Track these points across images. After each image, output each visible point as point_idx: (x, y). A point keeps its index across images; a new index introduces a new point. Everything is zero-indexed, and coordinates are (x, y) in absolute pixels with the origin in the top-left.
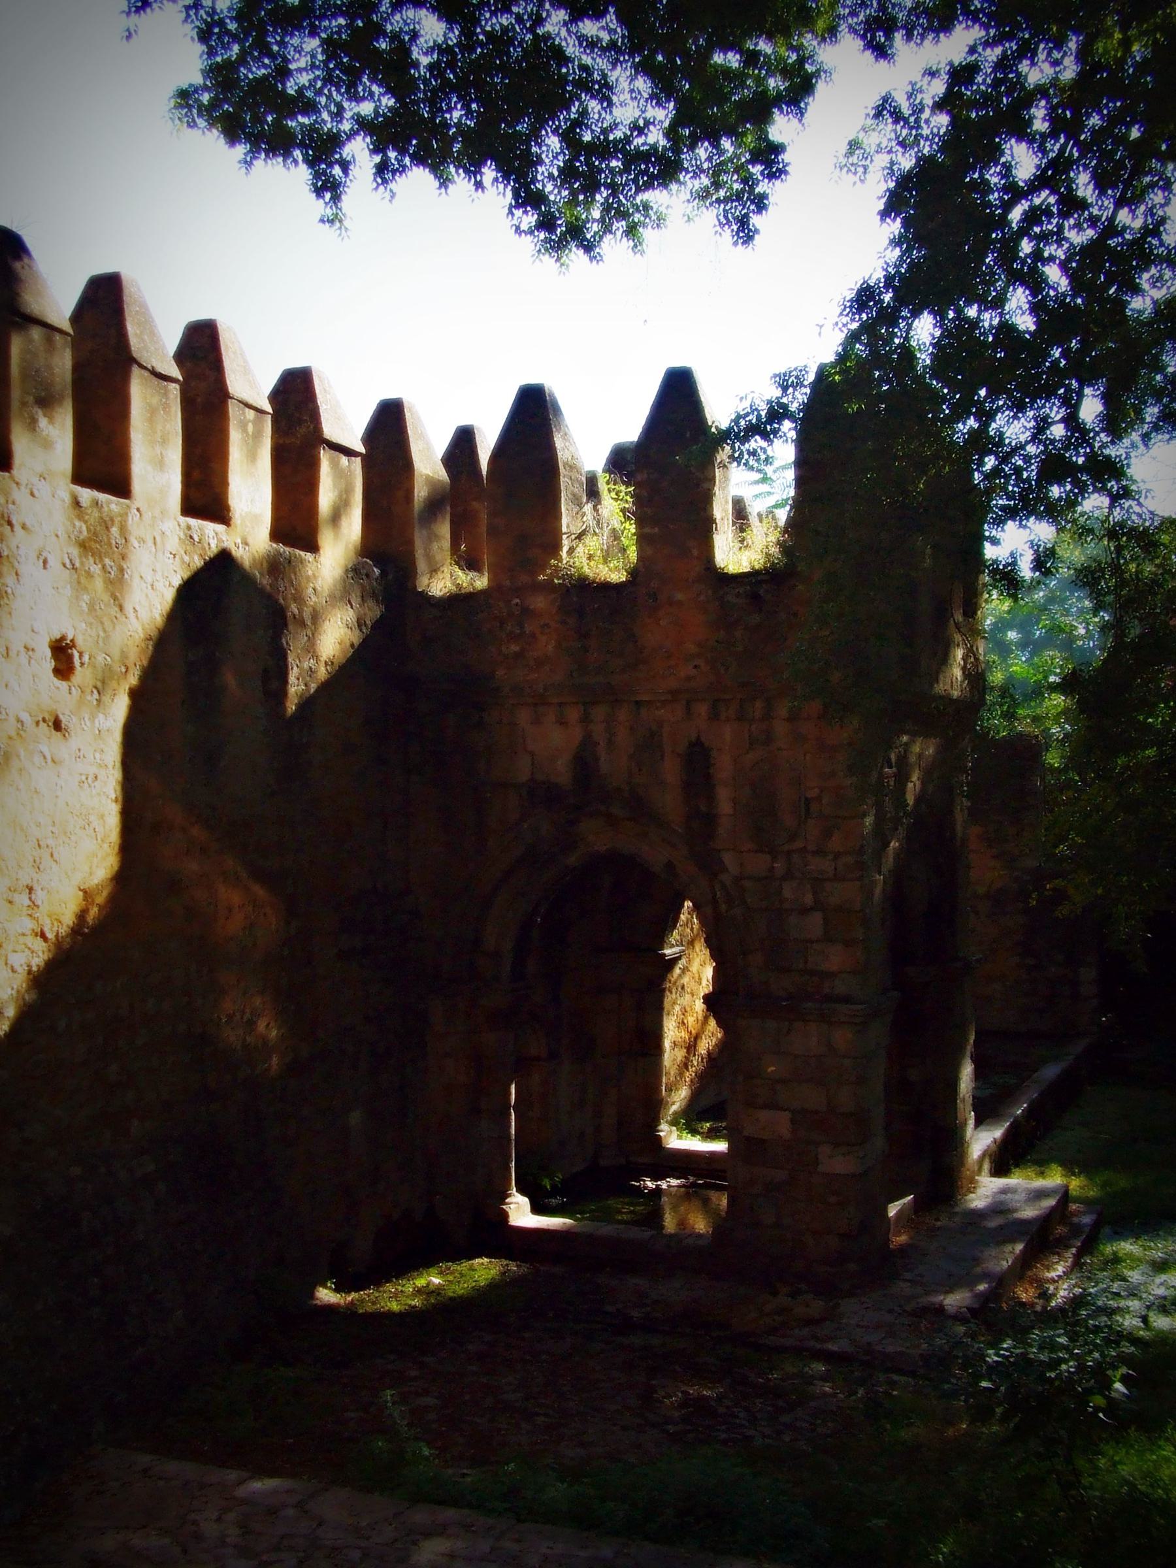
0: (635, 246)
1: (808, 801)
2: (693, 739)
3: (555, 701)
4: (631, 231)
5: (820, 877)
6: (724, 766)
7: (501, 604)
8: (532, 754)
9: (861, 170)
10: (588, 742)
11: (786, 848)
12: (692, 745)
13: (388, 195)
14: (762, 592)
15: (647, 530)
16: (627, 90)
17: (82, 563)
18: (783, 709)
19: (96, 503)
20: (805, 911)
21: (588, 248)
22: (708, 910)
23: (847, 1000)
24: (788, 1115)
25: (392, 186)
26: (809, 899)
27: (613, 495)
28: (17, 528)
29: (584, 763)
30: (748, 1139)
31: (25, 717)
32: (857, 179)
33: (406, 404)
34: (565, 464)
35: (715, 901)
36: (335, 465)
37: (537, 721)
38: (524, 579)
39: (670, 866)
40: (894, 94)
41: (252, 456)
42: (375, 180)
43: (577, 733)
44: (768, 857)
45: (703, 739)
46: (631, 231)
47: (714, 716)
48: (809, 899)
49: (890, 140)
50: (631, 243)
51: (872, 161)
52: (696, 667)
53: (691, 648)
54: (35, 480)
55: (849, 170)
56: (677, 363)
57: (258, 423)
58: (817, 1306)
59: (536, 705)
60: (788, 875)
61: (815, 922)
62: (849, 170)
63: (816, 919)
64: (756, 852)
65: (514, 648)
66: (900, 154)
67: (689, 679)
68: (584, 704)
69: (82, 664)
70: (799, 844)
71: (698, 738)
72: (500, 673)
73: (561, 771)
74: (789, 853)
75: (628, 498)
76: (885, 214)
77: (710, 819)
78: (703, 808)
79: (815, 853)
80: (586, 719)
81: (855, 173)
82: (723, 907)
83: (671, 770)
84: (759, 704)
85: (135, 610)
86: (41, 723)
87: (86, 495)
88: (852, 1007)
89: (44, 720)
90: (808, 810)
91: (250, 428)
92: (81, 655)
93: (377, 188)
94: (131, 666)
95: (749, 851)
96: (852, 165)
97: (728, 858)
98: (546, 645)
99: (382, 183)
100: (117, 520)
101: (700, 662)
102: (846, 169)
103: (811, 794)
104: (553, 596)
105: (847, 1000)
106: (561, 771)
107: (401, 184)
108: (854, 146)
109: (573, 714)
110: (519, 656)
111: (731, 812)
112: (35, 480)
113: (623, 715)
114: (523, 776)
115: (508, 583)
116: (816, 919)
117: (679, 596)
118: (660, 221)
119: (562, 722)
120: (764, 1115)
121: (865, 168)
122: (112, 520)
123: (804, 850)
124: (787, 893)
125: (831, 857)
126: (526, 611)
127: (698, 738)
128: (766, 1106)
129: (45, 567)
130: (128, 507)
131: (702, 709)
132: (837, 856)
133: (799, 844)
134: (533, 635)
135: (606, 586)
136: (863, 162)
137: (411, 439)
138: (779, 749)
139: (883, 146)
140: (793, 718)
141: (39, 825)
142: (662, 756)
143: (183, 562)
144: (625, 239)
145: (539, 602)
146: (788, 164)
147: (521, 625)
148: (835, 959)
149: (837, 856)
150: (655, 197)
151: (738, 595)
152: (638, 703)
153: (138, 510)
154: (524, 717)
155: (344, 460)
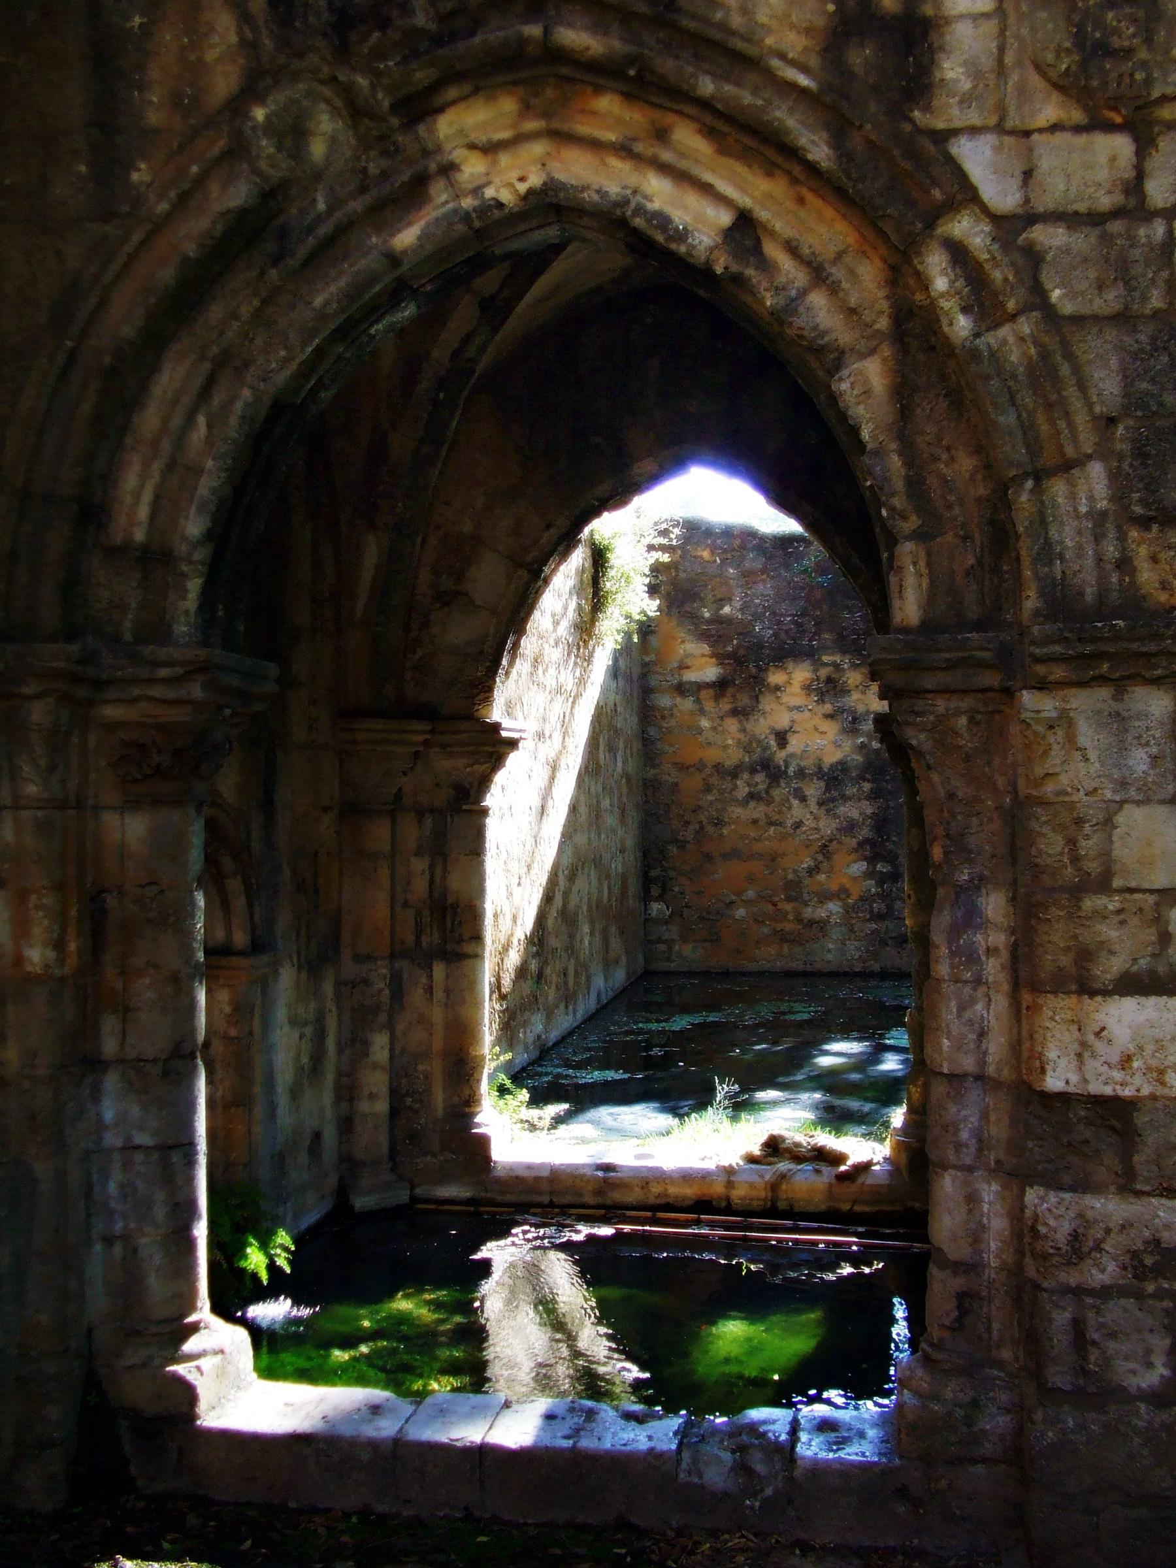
44: (1122, 145)
64: (1078, 129)
95: (1055, 128)
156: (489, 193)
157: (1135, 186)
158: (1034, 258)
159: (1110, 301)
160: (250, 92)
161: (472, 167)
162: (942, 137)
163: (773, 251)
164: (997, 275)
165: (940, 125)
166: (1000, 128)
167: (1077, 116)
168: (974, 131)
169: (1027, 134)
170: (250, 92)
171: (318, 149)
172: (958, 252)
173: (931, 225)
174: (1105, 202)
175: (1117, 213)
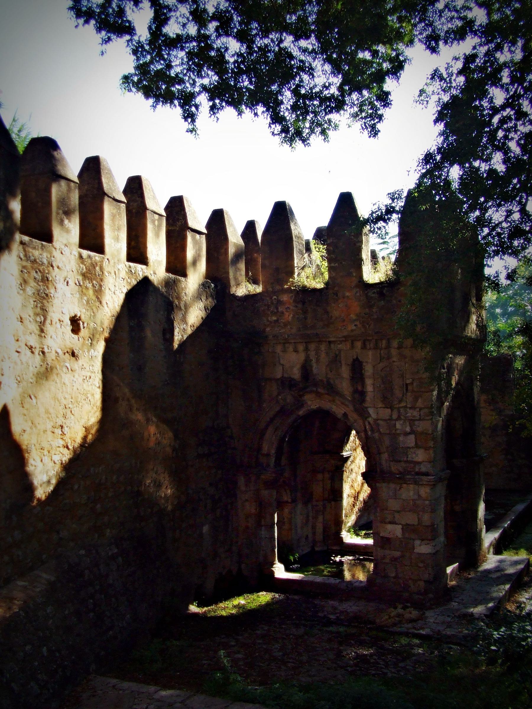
0: (325, 139)
1: (407, 385)
2: (355, 357)
3: (293, 341)
4: (323, 132)
5: (413, 418)
6: (368, 370)
7: (268, 299)
8: (283, 365)
9: (425, 102)
11: (397, 406)
12: (354, 360)
13: (216, 119)
14: (384, 291)
15: (332, 265)
16: (321, 70)
17: (84, 283)
19: (89, 257)
20: (406, 434)
21: (304, 141)
22: (363, 435)
23: (427, 474)
24: (400, 526)
25: (217, 115)
26: (408, 429)
27: (317, 249)
28: (55, 268)
29: (306, 369)
30: (382, 537)
31: (59, 351)
32: (423, 106)
33: (225, 212)
34: (296, 236)
35: (365, 431)
36: (194, 238)
37: (284, 351)
38: (278, 287)
39: (345, 415)
40: (439, 68)
41: (157, 235)
42: (210, 113)
43: (302, 356)
44: (389, 410)
45: (359, 358)
46: (323, 132)
47: (364, 347)
48: (408, 429)
49: (438, 89)
50: (323, 137)
51: (430, 98)
52: (355, 325)
53: (353, 316)
54: (63, 247)
55: (420, 103)
56: (345, 190)
57: (160, 220)
58: (415, 614)
60: (399, 418)
61: (411, 440)
62: (420, 103)
63: (412, 437)
65: (274, 318)
66: (443, 95)
67: (352, 331)
68: (306, 343)
69: (84, 327)
70: (403, 404)
71: (357, 358)
72: (268, 329)
73: (296, 374)
74: (399, 409)
75: (324, 251)
76: (436, 121)
77: (362, 394)
78: (360, 388)
79: (410, 408)
80: (306, 349)
81: (423, 104)
82: (369, 433)
83: (345, 372)
84: (384, 342)
85: (107, 303)
86: (66, 354)
87: (85, 253)
88: (429, 477)
89: (67, 352)
90: (407, 390)
91: (156, 223)
92: (83, 324)
93: (210, 117)
94: (105, 328)
95: (381, 408)
96: (421, 100)
97: (371, 411)
98: (288, 317)
99: (213, 114)
100: (99, 264)
101: (357, 323)
102: (418, 102)
103: (408, 382)
104: (291, 295)
105: (427, 474)
107: (221, 114)
108: (422, 92)
109: (301, 348)
110: (277, 321)
112: (63, 247)
113: (323, 347)
114: (279, 376)
115: (271, 289)
116: (412, 437)
117: (347, 294)
118: (336, 127)
119: (296, 351)
120: (390, 527)
121: (427, 101)
122: (96, 264)
123: (406, 407)
124: (398, 426)
125: (418, 410)
126: (280, 302)
127: (357, 358)
128: (390, 523)
129: (67, 285)
130: (103, 258)
131: (359, 344)
132: (421, 409)
133: (403, 404)
134: (283, 313)
135: (315, 290)
136: (426, 99)
137: (227, 227)
138: (394, 362)
139: (435, 91)
140: (400, 347)
141: (65, 398)
142: (341, 366)
143: (128, 282)
144: (320, 136)
145: (285, 298)
146: (392, 101)
147: (277, 309)
148: (420, 456)
149: (421, 409)
150: (334, 117)
151: (374, 293)
152: (330, 342)
153: (108, 259)
154: (279, 349)
155: (198, 236)
156: (312, 407)
157: (391, 416)
158: (378, 425)
159: (388, 432)
160: (279, 394)
161: (309, 403)
162: (367, 408)
163: (350, 418)
164: (374, 427)
165: (366, 406)
166: (374, 407)
167: (384, 406)
168: (370, 407)
170: (279, 394)
171: (288, 401)
172: (369, 423)
173: (366, 419)
174: (387, 418)
175: (389, 419)
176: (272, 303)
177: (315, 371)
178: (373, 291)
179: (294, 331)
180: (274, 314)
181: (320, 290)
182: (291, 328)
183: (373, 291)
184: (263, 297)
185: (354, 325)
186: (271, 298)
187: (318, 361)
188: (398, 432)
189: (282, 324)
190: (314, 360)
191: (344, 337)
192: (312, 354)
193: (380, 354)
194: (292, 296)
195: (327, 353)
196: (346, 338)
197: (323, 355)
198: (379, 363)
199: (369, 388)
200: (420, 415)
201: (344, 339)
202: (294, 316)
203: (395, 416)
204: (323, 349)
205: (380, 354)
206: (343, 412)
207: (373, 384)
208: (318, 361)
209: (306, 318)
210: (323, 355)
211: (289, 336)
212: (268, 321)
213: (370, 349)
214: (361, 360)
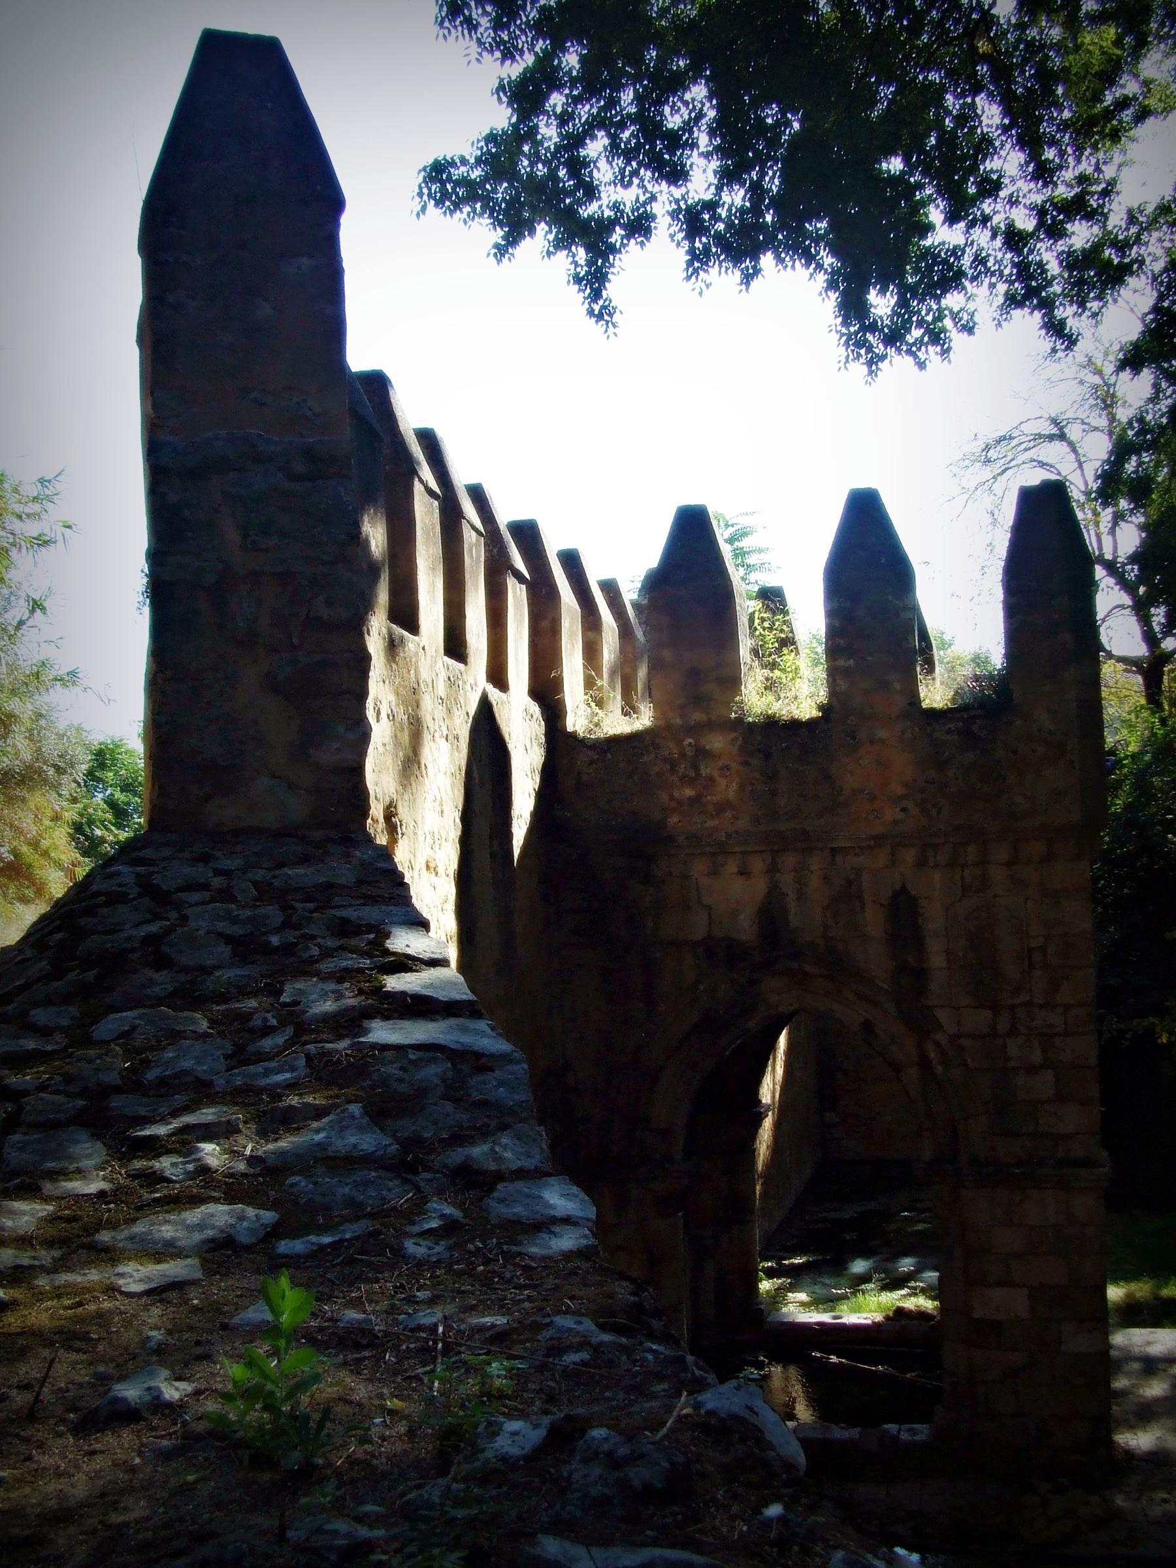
1: (1030, 950)
2: (898, 887)
6: (933, 918)
7: (671, 745)
8: (709, 908)
10: (774, 895)
14: (975, 728)
15: (841, 662)
18: (1000, 854)
20: (1032, 1069)
23: (1087, 1163)
26: (1037, 1057)
37: (714, 873)
38: (697, 716)
39: (868, 1027)
44: (987, 1014)
47: (921, 863)
48: (1037, 1057)
52: (903, 810)
56: (862, 484)
59: (714, 854)
60: (1013, 1031)
61: (1044, 1085)
63: (1048, 1075)
64: (975, 1007)
65: (689, 792)
67: (896, 822)
69: (403, 834)
72: (674, 820)
73: (745, 928)
74: (1012, 1008)
77: (920, 974)
79: (1041, 1006)
80: (772, 870)
83: (873, 921)
97: (943, 1016)
98: (728, 789)
101: (910, 805)
103: (1034, 944)
104: (734, 735)
105: (1087, 1163)
106: (745, 928)
109: (758, 864)
110: (696, 800)
111: (944, 965)
113: (816, 863)
115: (678, 721)
116: (1048, 1075)
117: (882, 734)
119: (744, 873)
126: (702, 753)
131: (909, 856)
138: (995, 896)
142: (863, 907)
145: (717, 742)
147: (696, 767)
151: (949, 732)
152: (833, 850)
154: (699, 868)
169: (959, 1008)
172: (938, 1045)
176: (683, 755)
177: (794, 920)
178: (947, 727)
179: (743, 823)
180: (687, 781)
181: (812, 722)
182: (735, 818)
183: (947, 727)
184: (657, 741)
185: (898, 809)
186: (679, 743)
187: (801, 896)
188: (1012, 1064)
189: (711, 808)
190: (792, 895)
191: (875, 838)
192: (786, 880)
193: (962, 877)
194: (736, 739)
195: (826, 878)
196: (878, 841)
197: (815, 881)
198: (960, 900)
199: (937, 961)
200: (1065, 1023)
201: (872, 843)
202: (742, 788)
203: (1002, 1028)
204: (814, 867)
205: (962, 877)
206: (862, 1020)
207: (948, 952)
208: (801, 896)
209: (774, 793)
210: (815, 881)
211: (728, 836)
212: (672, 798)
213: (936, 866)
214: (913, 893)
